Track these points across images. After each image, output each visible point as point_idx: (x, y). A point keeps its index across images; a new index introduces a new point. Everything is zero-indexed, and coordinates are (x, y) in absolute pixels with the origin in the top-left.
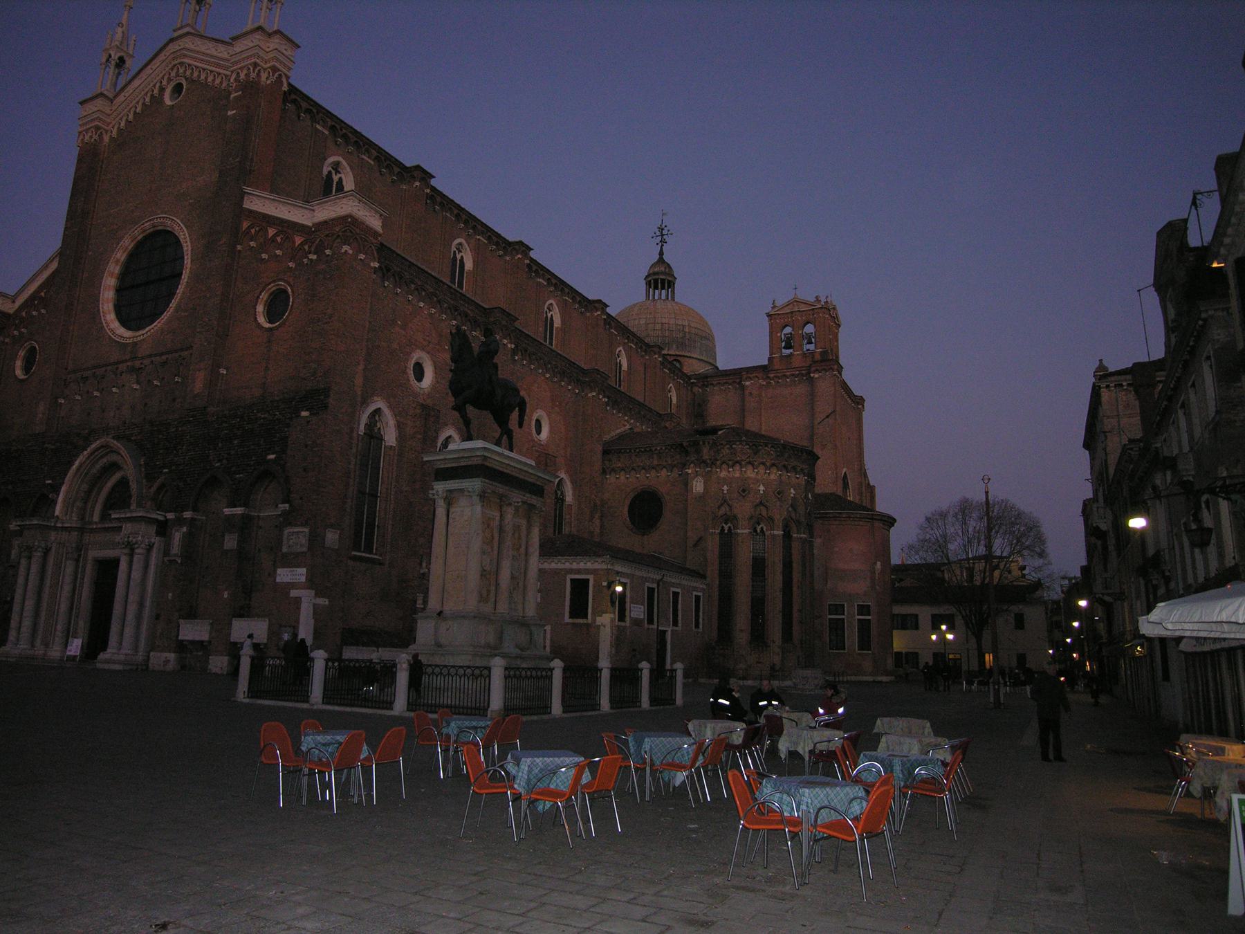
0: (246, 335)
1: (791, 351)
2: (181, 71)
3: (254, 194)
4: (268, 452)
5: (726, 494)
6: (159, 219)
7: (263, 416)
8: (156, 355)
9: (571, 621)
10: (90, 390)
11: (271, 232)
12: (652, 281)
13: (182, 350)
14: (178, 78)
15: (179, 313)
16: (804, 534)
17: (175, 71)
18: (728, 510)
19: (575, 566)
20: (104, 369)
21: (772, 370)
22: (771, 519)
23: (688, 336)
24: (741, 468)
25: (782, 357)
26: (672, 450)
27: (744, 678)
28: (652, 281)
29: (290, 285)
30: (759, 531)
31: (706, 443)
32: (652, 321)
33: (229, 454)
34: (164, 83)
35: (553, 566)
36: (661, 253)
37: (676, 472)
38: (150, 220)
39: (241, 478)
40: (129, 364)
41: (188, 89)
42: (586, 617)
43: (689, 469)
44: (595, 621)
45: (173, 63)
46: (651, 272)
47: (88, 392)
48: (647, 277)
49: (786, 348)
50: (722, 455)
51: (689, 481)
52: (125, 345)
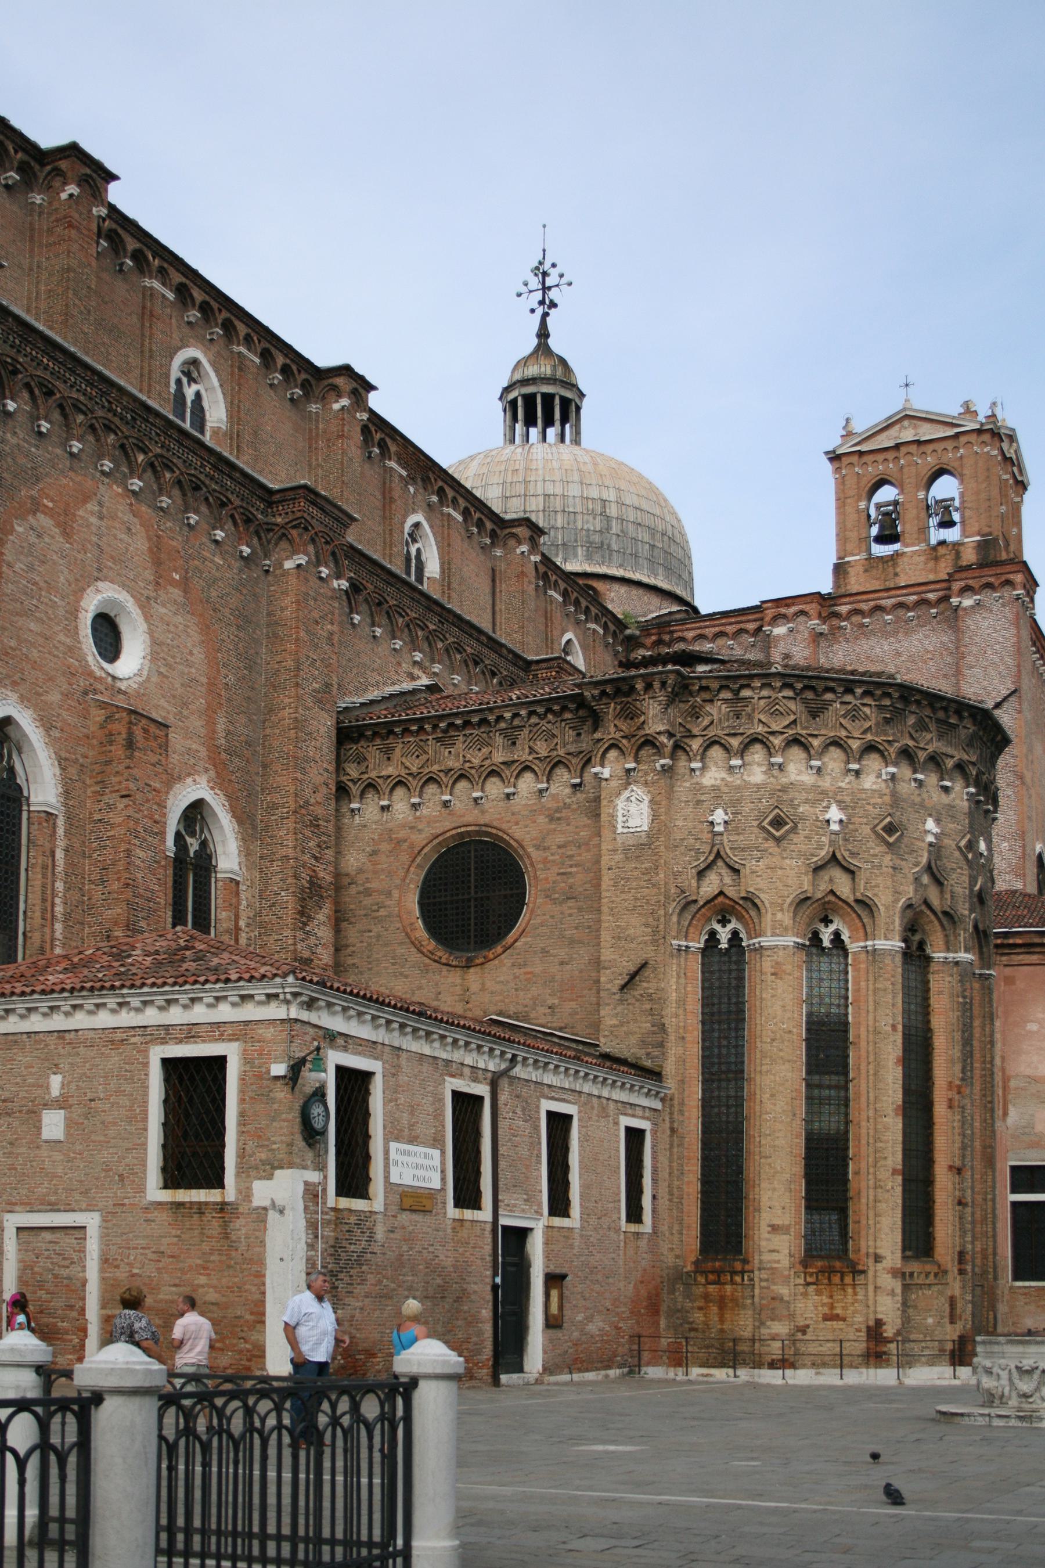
1: (897, 546)
5: (721, 834)
9: (166, 1196)
12: (520, 400)
16: (967, 951)
18: (728, 880)
19: (176, 1016)
21: (845, 596)
22: (865, 904)
23: (615, 528)
24: (770, 755)
25: (872, 562)
26: (550, 717)
27: (783, 1363)
28: (520, 400)
30: (826, 943)
31: (657, 685)
32: (520, 489)
35: (104, 1019)
36: (543, 334)
37: (563, 781)
42: (218, 1182)
43: (602, 766)
44: (246, 1194)
46: (515, 378)
48: (507, 390)
49: (881, 539)
50: (706, 722)
51: (604, 803)
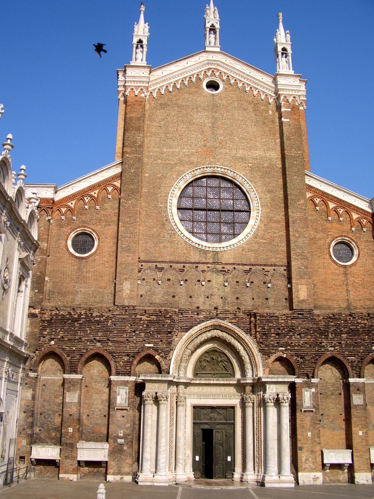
0: (325, 266)
2: (217, 74)
3: (311, 177)
4: (372, 345)
6: (219, 169)
7: (362, 322)
8: (239, 264)
10: (171, 279)
11: (332, 205)
13: (265, 265)
14: (213, 77)
15: (257, 239)
17: (210, 72)
20: (182, 265)
29: (354, 241)
33: (340, 343)
34: (201, 77)
38: (210, 167)
39: (352, 359)
40: (209, 265)
41: (225, 89)
45: (208, 67)
47: (169, 280)
52: (206, 252)
